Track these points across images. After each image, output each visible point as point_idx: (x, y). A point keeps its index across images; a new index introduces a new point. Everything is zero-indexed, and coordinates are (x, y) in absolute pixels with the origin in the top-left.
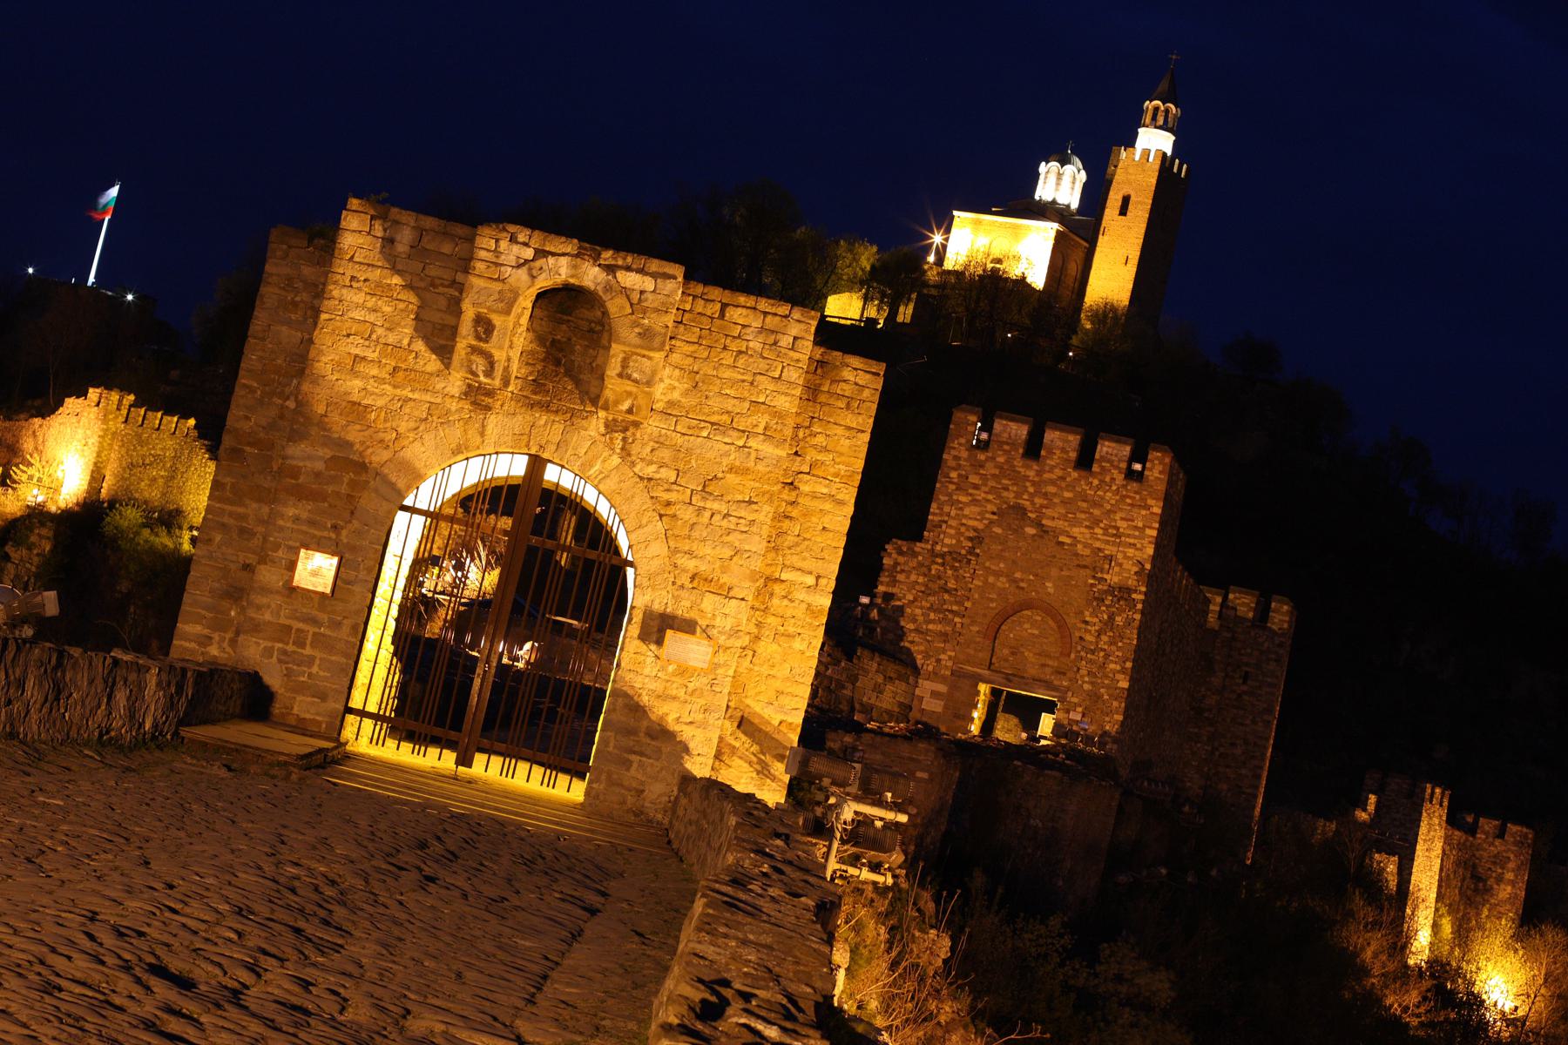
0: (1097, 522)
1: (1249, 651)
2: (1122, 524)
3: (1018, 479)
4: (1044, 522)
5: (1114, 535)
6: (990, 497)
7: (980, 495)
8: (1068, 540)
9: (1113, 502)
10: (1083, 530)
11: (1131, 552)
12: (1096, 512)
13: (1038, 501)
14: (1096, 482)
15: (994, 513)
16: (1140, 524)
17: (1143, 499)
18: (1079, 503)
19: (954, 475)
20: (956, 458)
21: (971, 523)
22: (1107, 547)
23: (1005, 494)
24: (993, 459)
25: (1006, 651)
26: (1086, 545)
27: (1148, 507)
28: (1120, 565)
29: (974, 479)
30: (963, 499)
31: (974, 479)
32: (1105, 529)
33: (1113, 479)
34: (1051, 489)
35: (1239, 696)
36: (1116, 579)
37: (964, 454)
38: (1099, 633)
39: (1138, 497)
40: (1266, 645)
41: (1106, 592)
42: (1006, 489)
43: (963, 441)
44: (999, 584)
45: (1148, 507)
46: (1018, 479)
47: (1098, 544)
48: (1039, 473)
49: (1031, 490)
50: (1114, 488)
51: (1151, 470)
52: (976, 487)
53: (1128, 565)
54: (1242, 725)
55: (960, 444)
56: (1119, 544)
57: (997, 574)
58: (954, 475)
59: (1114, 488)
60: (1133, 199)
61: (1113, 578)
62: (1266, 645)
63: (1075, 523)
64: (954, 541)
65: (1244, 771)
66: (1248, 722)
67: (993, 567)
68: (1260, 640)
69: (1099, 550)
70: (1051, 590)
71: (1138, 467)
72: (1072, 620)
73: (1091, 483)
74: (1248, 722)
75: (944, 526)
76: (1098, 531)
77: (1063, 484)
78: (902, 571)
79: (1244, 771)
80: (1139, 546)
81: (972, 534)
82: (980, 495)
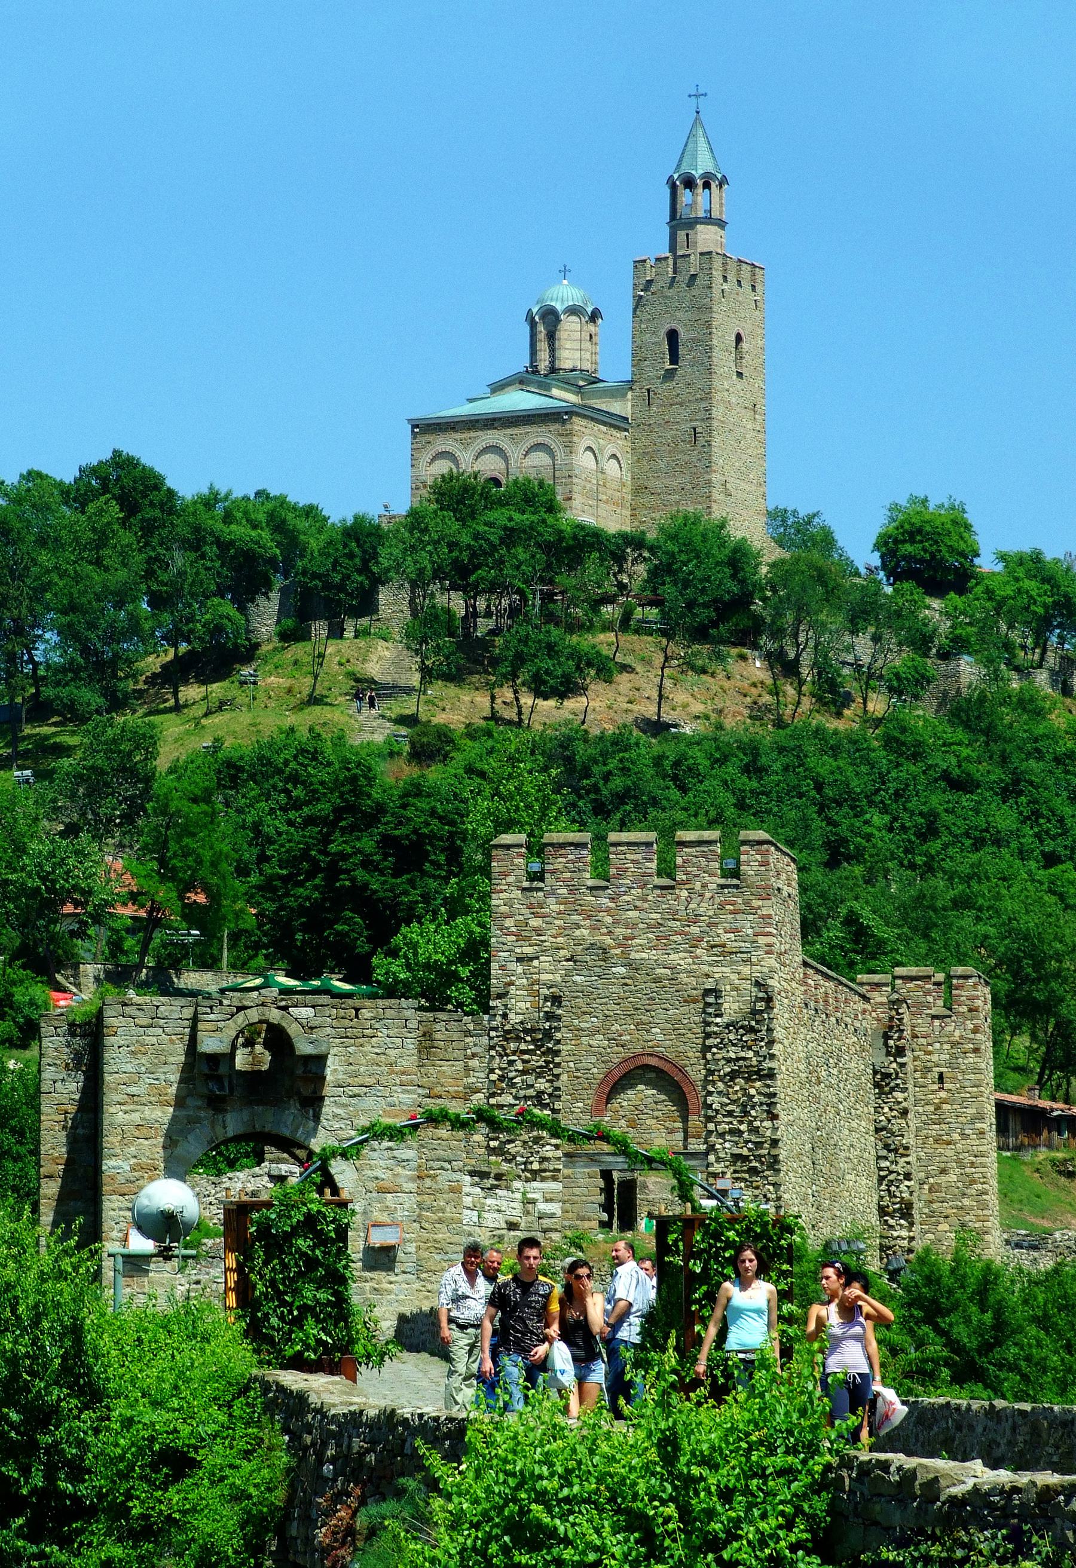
0: (694, 943)
1: (937, 1045)
4: (634, 955)
5: (722, 954)
6: (560, 940)
7: (548, 940)
8: (668, 972)
9: (711, 913)
10: (682, 955)
11: (746, 970)
12: (694, 929)
13: (620, 931)
14: (685, 893)
15: (567, 960)
16: (750, 932)
17: (747, 903)
18: (672, 924)
19: (509, 922)
20: (509, 903)
21: (544, 977)
22: (716, 969)
23: (577, 933)
24: (553, 893)
25: (623, 1123)
28: (737, 989)
29: (534, 922)
30: (529, 950)
31: (534, 922)
33: (704, 886)
34: (633, 914)
35: (938, 1108)
36: (735, 1006)
39: (740, 901)
40: (957, 1033)
41: (728, 1026)
42: (578, 927)
43: (511, 879)
44: (594, 1043)
47: (706, 968)
48: (612, 899)
49: (609, 920)
50: (708, 895)
51: (748, 863)
52: (539, 932)
54: (948, 1143)
55: (508, 884)
56: (733, 963)
57: (593, 1033)
58: (509, 922)
59: (708, 895)
60: (683, 336)
61: (732, 1007)
62: (957, 1033)
64: (528, 1005)
65: (966, 1202)
66: (956, 1136)
67: (584, 1025)
68: (948, 1028)
69: (708, 976)
70: (660, 1037)
73: (678, 897)
74: (956, 1136)
75: (512, 990)
76: (699, 951)
77: (646, 905)
78: (474, 1055)
79: (966, 1202)
80: (754, 959)
81: (545, 991)
82: (548, 940)
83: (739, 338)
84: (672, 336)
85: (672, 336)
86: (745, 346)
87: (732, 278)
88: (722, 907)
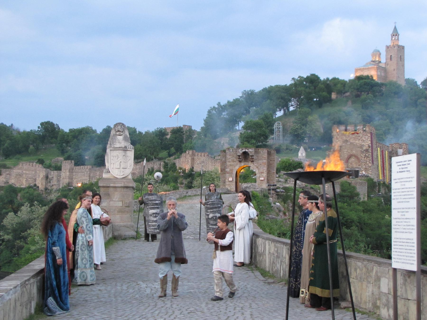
2: (364, 139)
3: (345, 135)
11: (366, 143)
12: (359, 138)
25: (350, 164)
26: (359, 144)
27: (367, 135)
31: (338, 137)
32: (361, 140)
36: (365, 148)
37: (336, 133)
38: (364, 158)
45: (367, 135)
46: (345, 135)
47: (361, 143)
53: (366, 145)
60: (393, 56)
61: (364, 148)
63: (356, 141)
71: (364, 129)
72: (359, 157)
83: (401, 56)
84: (391, 56)
85: (391, 56)
86: (402, 57)
88: (363, 135)
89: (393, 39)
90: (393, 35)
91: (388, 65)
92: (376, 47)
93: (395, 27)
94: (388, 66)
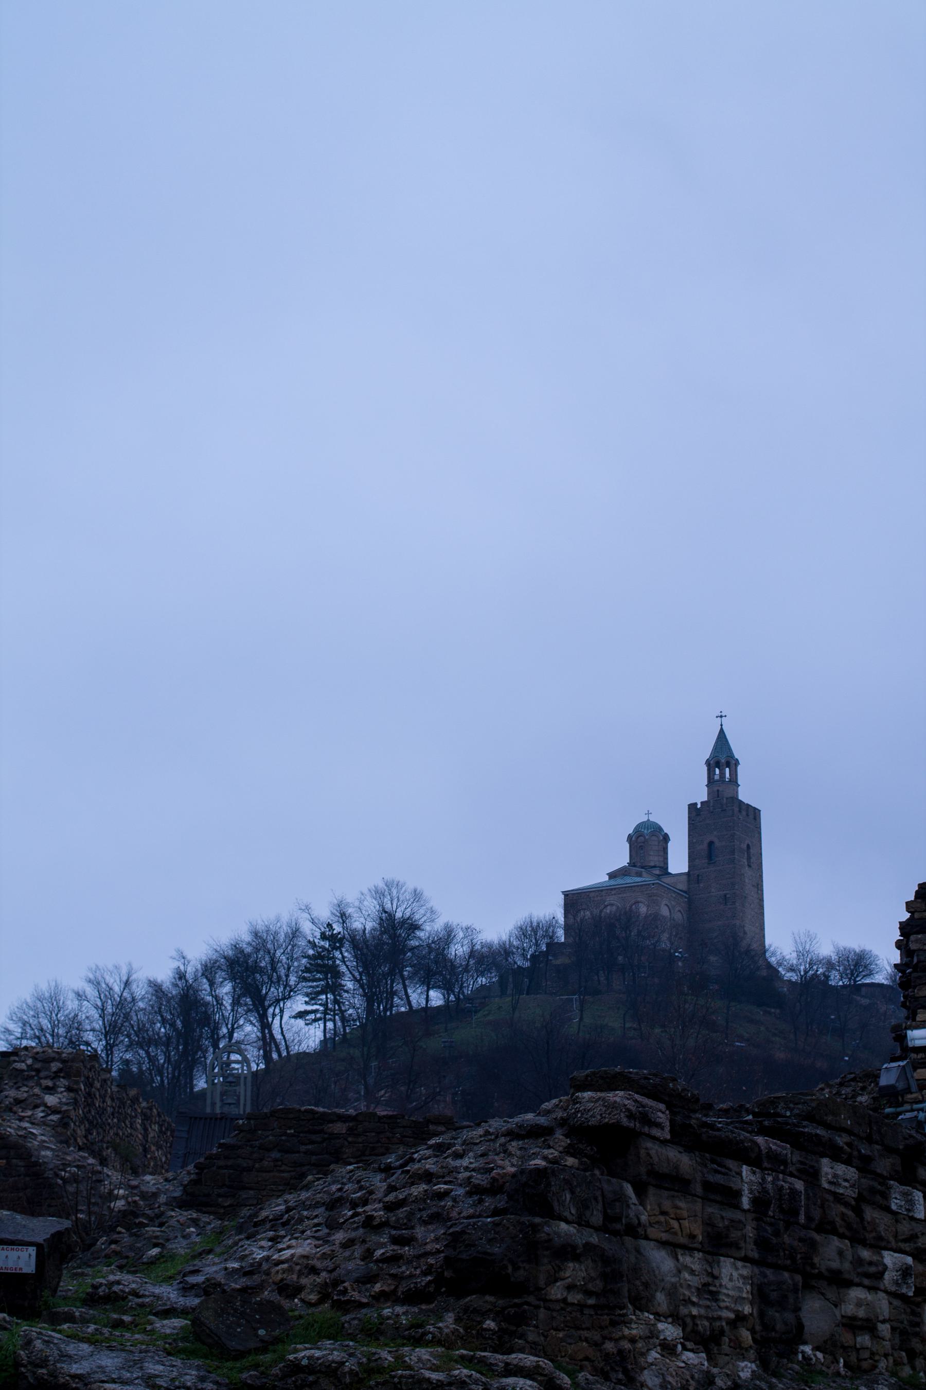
60: (717, 843)
83: (748, 846)
84: (711, 844)
85: (711, 844)
87: (744, 813)
89: (717, 777)
90: (713, 764)
91: (698, 882)
92: (648, 813)
93: (722, 732)
94: (702, 885)
